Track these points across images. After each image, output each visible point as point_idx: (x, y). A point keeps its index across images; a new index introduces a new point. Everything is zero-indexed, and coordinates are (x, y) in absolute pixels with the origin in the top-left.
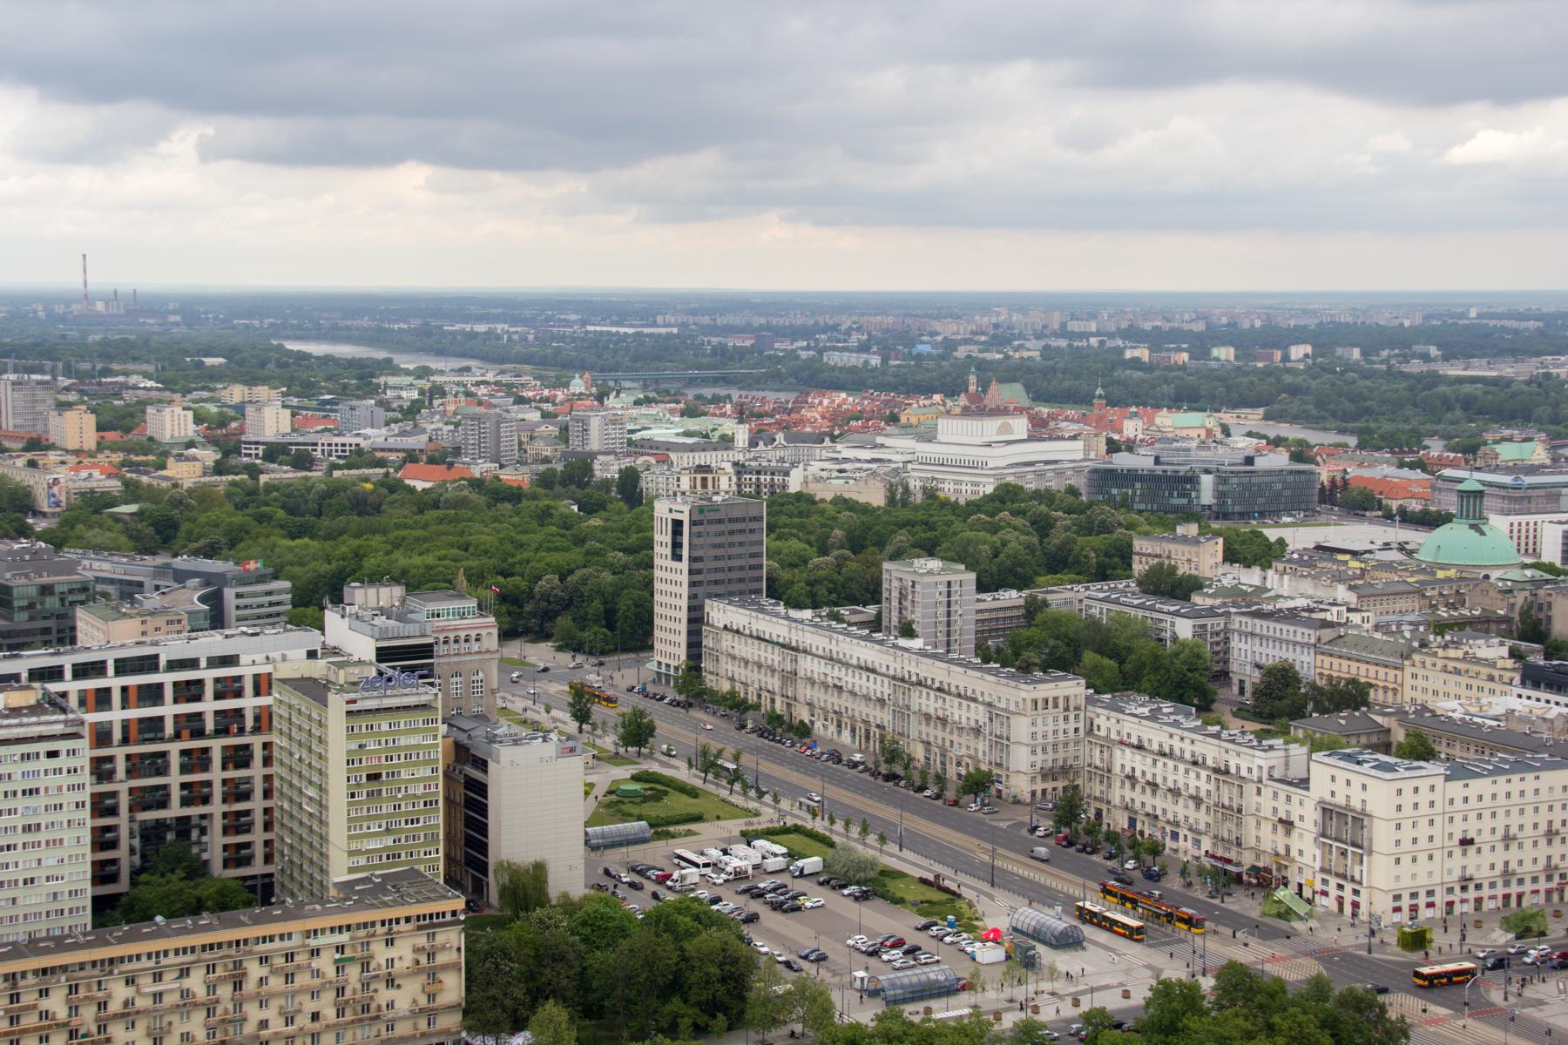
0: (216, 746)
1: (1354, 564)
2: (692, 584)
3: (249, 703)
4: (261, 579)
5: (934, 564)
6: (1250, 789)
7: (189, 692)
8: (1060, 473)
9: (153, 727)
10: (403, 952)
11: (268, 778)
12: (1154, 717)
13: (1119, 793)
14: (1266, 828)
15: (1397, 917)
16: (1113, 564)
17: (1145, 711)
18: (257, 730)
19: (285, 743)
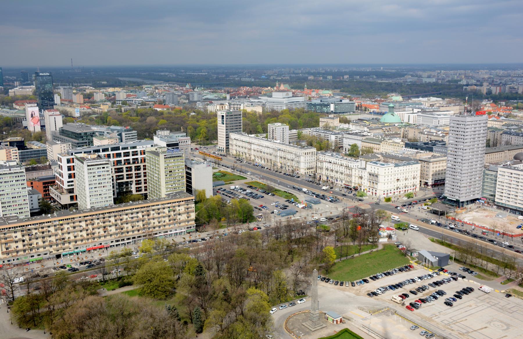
0: (133, 166)
1: (367, 123)
2: (226, 129)
3: (139, 157)
4: (130, 131)
5: (280, 124)
6: (353, 170)
7: (127, 154)
8: (300, 104)
9: (119, 162)
10: (182, 209)
11: (145, 173)
12: (332, 156)
13: (324, 172)
14: (357, 178)
15: (384, 196)
16: (316, 124)
17: (330, 154)
18: (141, 162)
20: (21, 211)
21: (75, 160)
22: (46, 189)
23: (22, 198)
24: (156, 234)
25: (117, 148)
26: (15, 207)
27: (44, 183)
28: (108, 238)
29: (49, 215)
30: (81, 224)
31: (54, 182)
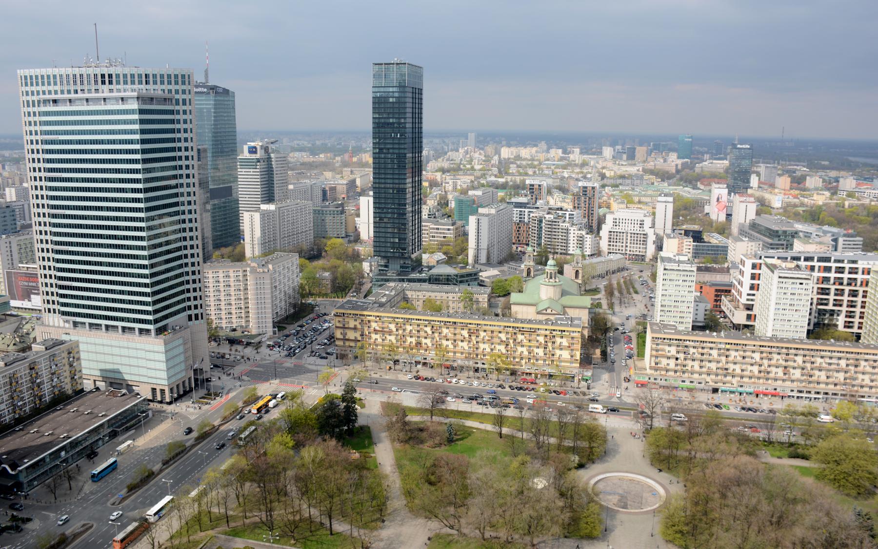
3: (860, 277)
4: (852, 236)
7: (840, 270)
9: (826, 280)
19: (873, 292)
20: (681, 320)
21: (763, 266)
22: (717, 300)
23: (686, 304)
24: (863, 397)
25: (828, 260)
26: (675, 314)
27: (716, 291)
28: (788, 383)
29: (715, 334)
30: (754, 355)
31: (730, 291)
